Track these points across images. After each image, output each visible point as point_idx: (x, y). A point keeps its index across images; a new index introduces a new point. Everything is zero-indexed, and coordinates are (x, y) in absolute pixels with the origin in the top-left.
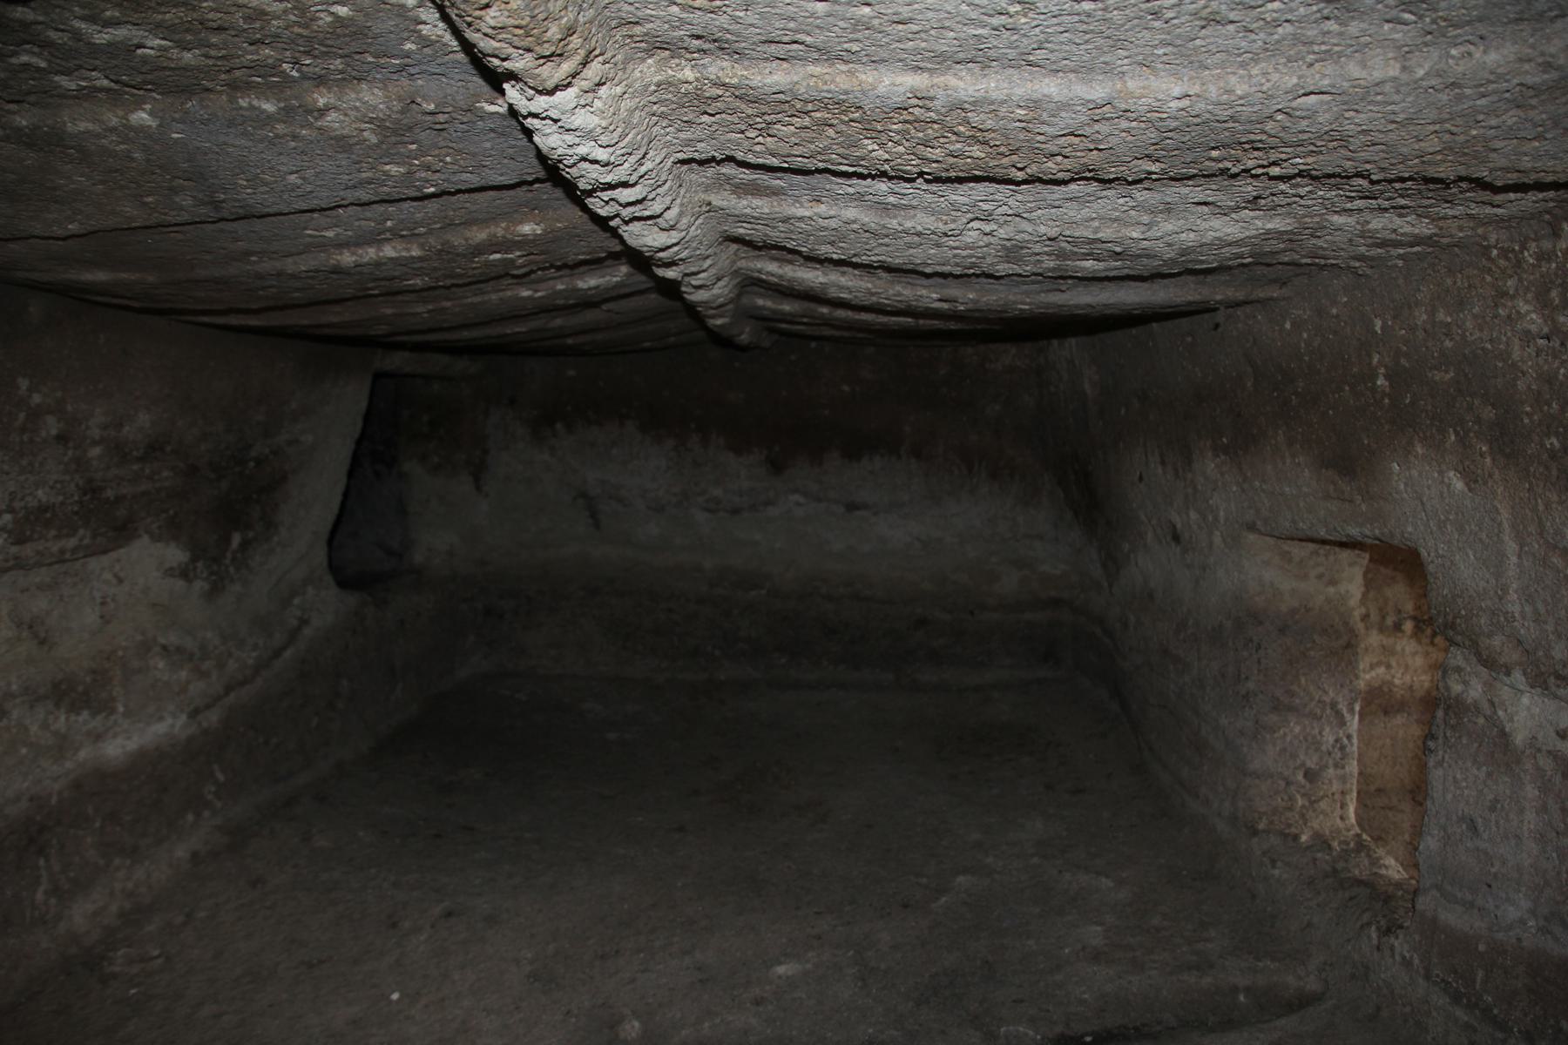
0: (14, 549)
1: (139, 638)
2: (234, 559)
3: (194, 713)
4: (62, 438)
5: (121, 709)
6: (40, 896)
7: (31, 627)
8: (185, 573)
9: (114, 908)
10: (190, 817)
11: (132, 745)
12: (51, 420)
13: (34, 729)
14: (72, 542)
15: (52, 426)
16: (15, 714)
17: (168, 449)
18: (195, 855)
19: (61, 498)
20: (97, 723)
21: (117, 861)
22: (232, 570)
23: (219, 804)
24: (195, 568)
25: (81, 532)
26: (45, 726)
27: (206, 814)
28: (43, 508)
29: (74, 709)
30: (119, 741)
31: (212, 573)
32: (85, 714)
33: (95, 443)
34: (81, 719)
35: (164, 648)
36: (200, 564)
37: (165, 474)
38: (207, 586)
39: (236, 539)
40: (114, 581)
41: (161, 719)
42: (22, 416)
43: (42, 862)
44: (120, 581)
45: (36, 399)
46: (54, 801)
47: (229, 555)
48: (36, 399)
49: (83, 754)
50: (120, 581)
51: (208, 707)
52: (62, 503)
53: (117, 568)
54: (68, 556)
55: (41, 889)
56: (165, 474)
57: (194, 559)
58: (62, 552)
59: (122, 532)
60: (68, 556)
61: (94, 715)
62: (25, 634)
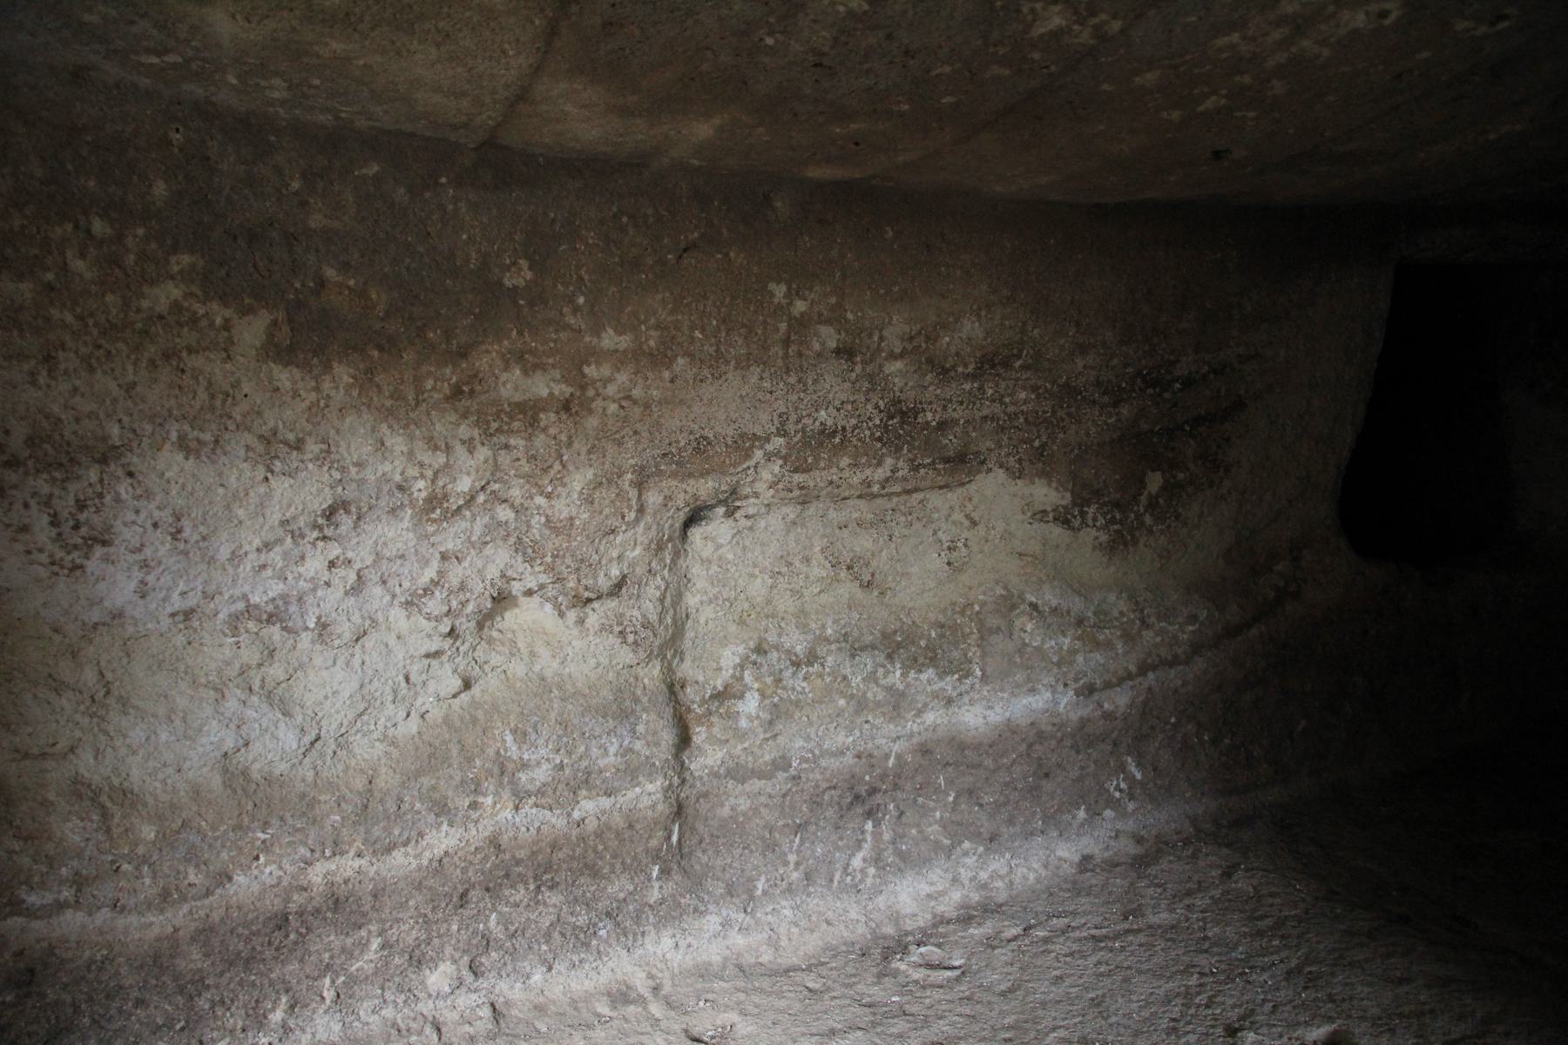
0: (798, 478)
1: (1000, 591)
2: (1152, 505)
3: (1089, 690)
5: (978, 673)
6: (857, 862)
7: (849, 568)
8: (1063, 518)
9: (956, 896)
10: (1082, 814)
11: (996, 716)
13: (856, 681)
14: (880, 473)
15: (829, 337)
16: (830, 660)
17: (1018, 364)
18: (1086, 858)
19: (854, 421)
20: (948, 684)
21: (967, 845)
22: (1148, 519)
23: (1131, 806)
24: (1083, 514)
25: (889, 461)
26: (872, 678)
27: (1108, 813)
28: (826, 433)
29: (914, 664)
30: (978, 709)
31: (1113, 521)
32: (930, 673)
33: (893, 357)
34: (924, 677)
35: (1034, 606)
36: (1091, 510)
37: (1023, 395)
38: (1104, 538)
39: (1154, 481)
40: (967, 523)
41: (1032, 691)
42: (783, 326)
43: (869, 826)
44: (974, 523)
45: (800, 306)
46: (891, 762)
47: (1143, 499)
48: (800, 306)
49: (930, 717)
50: (974, 523)
51: (1108, 685)
52: (855, 427)
53: (970, 507)
54: (875, 489)
55: (860, 855)
56: (1023, 395)
57: (1080, 502)
58: (867, 483)
59: (961, 464)
60: (875, 489)
61: (942, 675)
62: (843, 574)
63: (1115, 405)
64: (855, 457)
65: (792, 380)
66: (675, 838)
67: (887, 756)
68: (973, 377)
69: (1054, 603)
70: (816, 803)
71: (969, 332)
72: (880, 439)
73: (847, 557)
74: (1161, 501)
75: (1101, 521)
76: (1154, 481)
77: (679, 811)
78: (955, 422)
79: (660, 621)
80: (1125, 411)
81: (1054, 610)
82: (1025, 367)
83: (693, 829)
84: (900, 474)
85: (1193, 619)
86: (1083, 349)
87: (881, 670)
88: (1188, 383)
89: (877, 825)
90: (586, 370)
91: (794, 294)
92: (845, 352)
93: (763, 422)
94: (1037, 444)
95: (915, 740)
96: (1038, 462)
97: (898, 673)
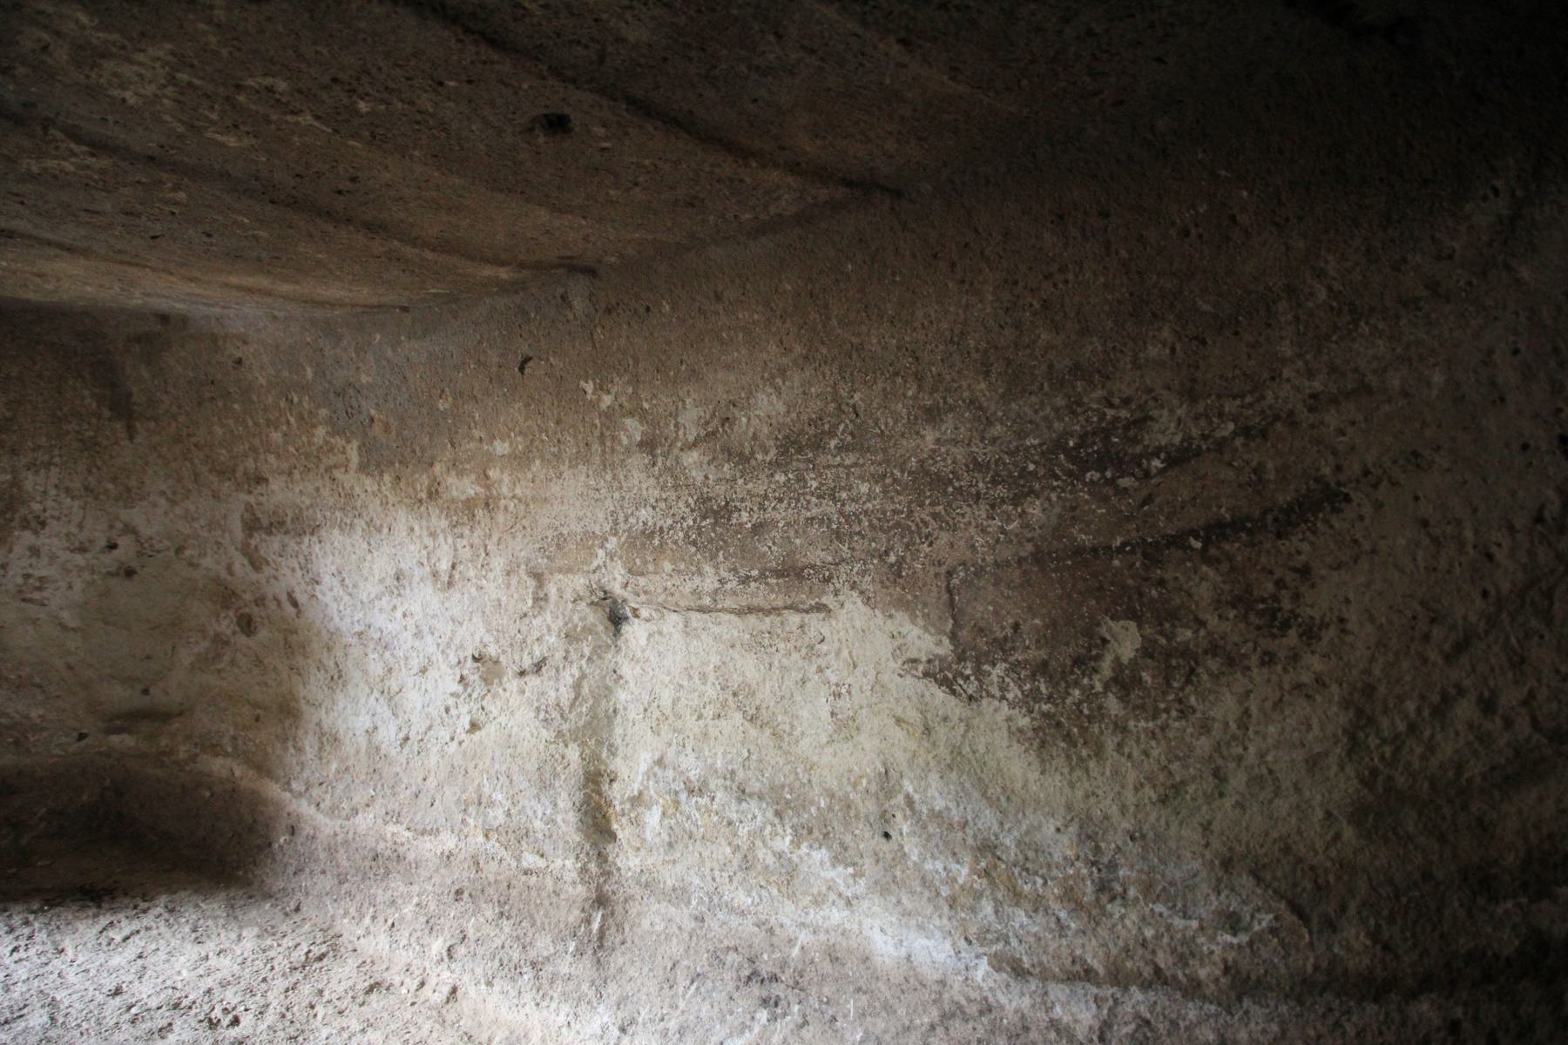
4: (648, 445)
7: (735, 694)
12: (630, 422)
15: (634, 429)
17: (833, 443)
19: (670, 522)
22: (1113, 704)
29: (802, 833)
31: (1034, 695)
37: (864, 488)
45: (607, 400)
48: (607, 400)
52: (671, 528)
58: (696, 593)
60: (707, 601)
61: (836, 860)
63: (1016, 501)
64: (673, 561)
65: (609, 477)
66: (596, 926)
67: (791, 942)
68: (776, 465)
69: (939, 804)
70: (717, 958)
71: (767, 409)
72: (694, 543)
73: (736, 680)
74: (1146, 677)
75: (1014, 693)
76: (1125, 641)
77: (601, 901)
78: (774, 523)
79: (572, 706)
80: (1035, 509)
81: (937, 816)
82: (843, 448)
83: (620, 928)
84: (728, 586)
85: (1233, 922)
86: (932, 415)
87: (769, 828)
88: (1178, 458)
89: (773, 1019)
90: (491, 473)
91: (601, 388)
92: (648, 445)
93: (601, 525)
94: (892, 559)
95: (822, 937)
96: (896, 585)
97: (788, 839)
